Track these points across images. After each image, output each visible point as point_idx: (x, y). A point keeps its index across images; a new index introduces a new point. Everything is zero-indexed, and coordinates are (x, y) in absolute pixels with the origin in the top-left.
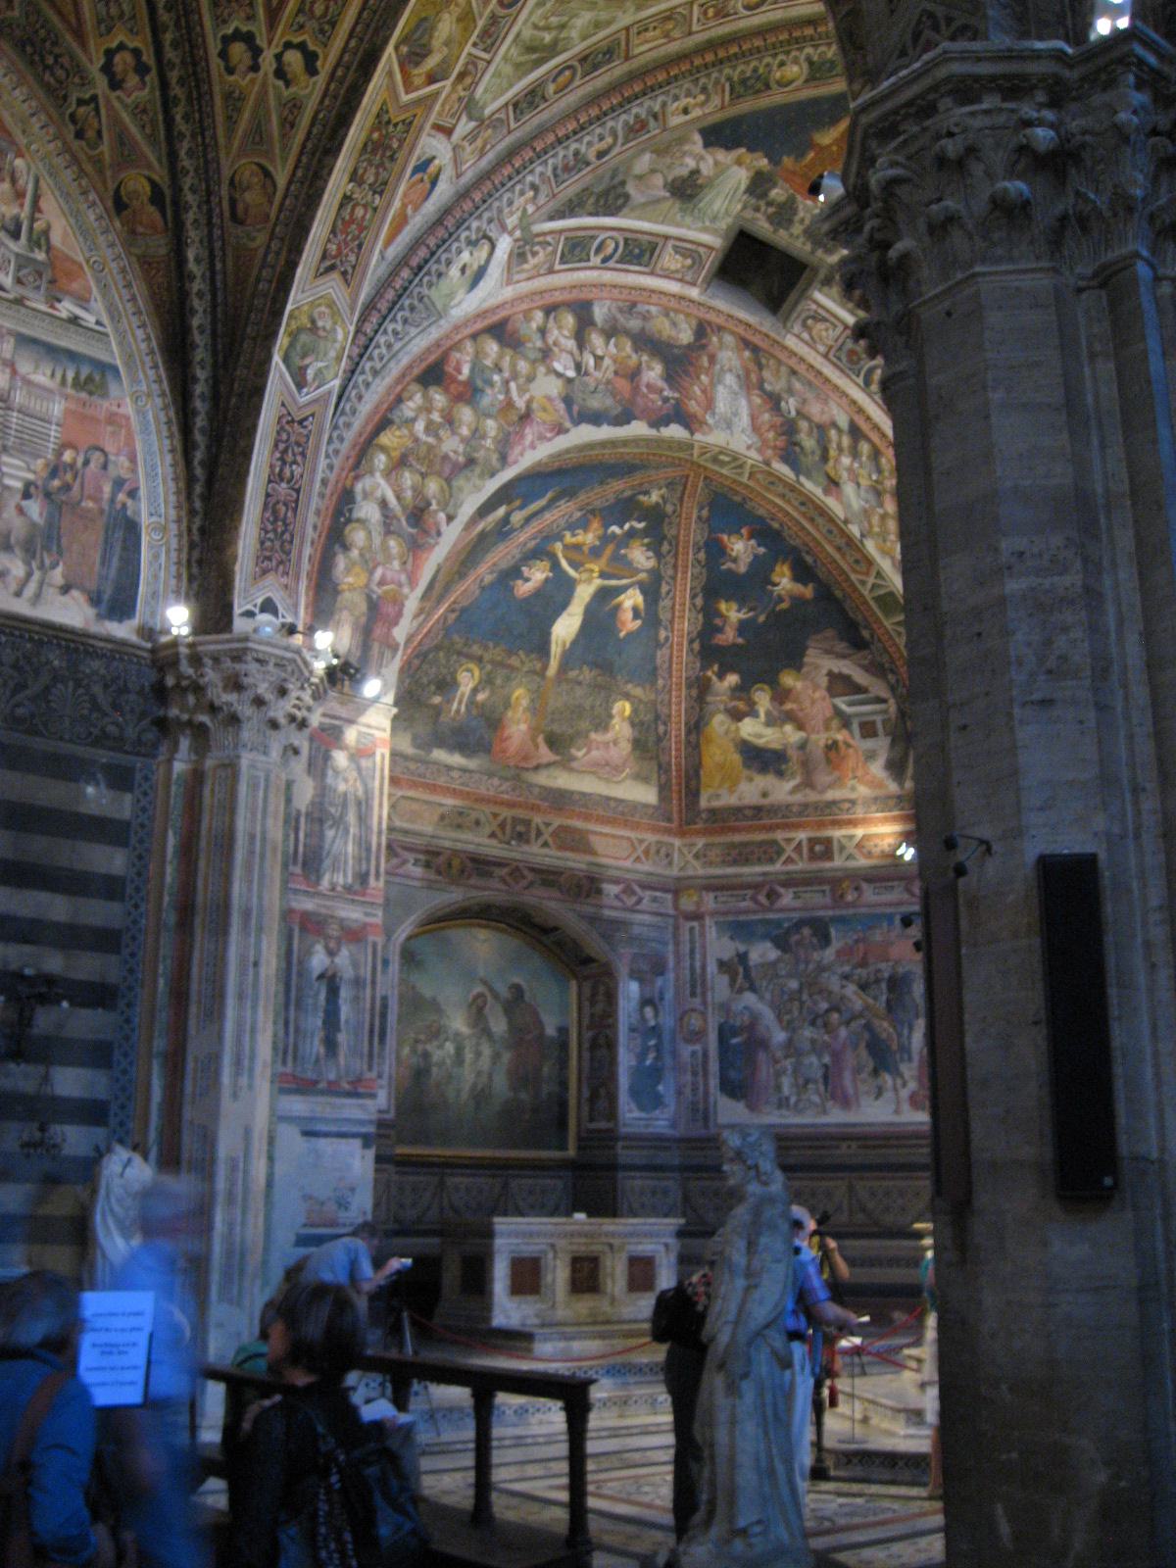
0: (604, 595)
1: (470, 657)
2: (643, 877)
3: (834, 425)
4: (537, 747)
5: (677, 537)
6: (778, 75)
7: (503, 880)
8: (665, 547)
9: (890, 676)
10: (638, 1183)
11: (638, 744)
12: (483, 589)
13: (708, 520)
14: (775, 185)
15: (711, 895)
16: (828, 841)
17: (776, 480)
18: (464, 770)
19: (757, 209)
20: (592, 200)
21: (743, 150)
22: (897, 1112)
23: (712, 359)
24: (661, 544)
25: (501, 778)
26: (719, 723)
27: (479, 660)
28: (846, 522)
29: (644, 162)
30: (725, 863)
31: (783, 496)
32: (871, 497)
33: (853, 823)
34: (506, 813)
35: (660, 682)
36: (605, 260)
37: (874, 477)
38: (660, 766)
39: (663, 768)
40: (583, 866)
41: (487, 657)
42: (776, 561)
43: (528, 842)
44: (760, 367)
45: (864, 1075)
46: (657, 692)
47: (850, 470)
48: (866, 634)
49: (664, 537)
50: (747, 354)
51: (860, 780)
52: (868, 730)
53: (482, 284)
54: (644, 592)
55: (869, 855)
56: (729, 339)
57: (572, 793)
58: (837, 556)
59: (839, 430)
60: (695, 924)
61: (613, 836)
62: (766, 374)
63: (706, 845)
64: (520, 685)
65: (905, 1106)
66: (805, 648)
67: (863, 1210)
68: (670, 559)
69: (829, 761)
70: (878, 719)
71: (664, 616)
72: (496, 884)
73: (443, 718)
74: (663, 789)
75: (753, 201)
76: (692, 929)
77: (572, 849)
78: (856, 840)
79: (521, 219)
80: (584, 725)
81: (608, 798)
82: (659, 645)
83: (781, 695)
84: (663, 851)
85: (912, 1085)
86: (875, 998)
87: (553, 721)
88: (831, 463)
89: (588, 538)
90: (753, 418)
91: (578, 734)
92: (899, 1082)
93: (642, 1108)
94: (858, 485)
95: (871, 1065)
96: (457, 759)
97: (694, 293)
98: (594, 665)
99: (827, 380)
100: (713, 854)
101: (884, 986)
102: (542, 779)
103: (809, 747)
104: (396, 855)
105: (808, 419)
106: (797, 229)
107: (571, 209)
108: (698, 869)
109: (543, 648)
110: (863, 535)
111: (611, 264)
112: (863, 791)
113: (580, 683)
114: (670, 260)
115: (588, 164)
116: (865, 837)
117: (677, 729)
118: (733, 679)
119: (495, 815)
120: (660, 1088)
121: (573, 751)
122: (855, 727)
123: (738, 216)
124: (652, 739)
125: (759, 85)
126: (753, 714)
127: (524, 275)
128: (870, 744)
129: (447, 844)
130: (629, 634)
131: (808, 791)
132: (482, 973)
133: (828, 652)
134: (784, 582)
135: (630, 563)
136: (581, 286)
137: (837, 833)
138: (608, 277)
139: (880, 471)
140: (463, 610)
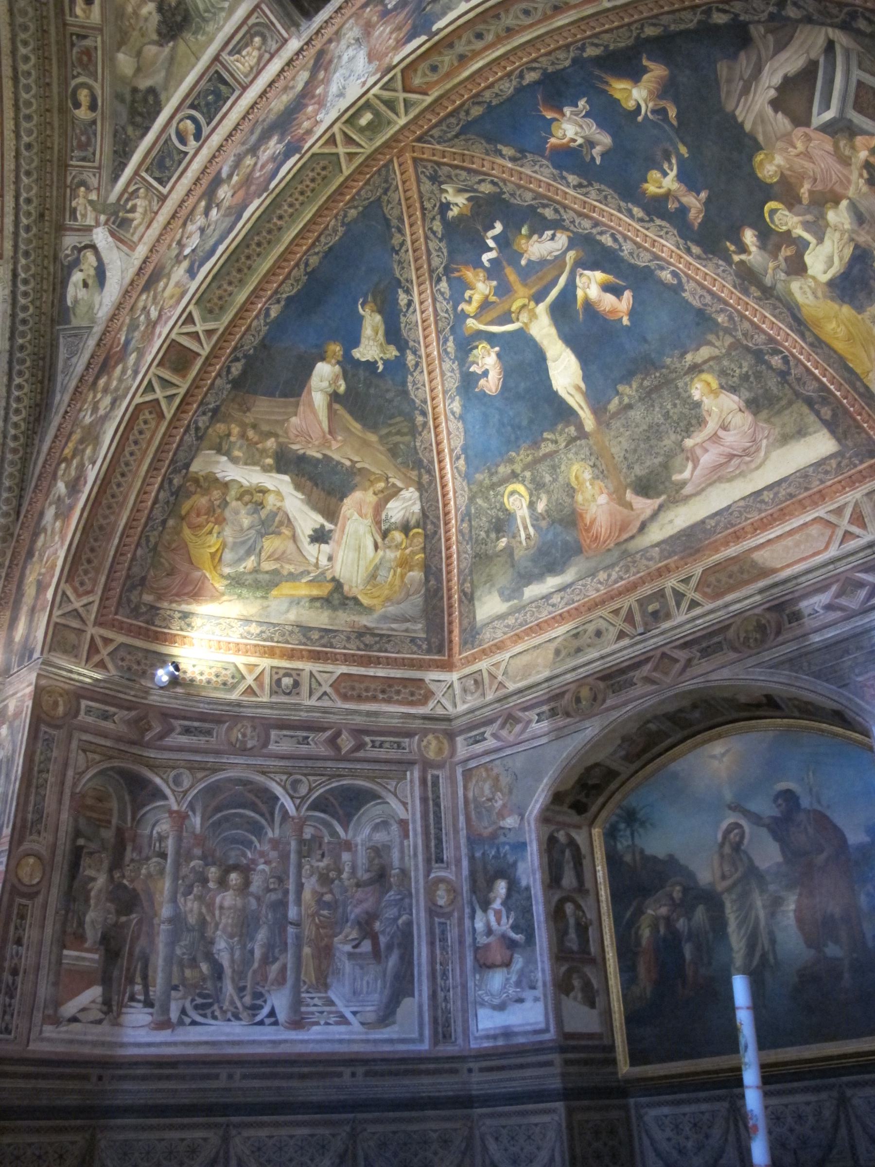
0: (563, 311)
1: (505, 481)
4: (629, 506)
5: (537, 196)
7: (648, 680)
8: (548, 213)
11: (754, 405)
12: (461, 418)
13: (522, 151)
18: (562, 589)
20: (130, 130)
24: (543, 217)
25: (606, 568)
27: (514, 476)
29: (125, 62)
31: (463, 59)
34: (629, 601)
36: (197, 136)
38: (810, 402)
40: (758, 598)
41: (518, 468)
42: (605, 92)
43: (668, 616)
46: (727, 331)
49: (532, 209)
53: (108, 274)
57: (703, 522)
61: (790, 533)
64: (569, 467)
66: (734, 117)
71: (642, 261)
72: (640, 689)
73: (519, 554)
77: (731, 589)
79: (95, 209)
80: (669, 441)
81: (759, 493)
82: (678, 288)
83: (786, 191)
87: (630, 467)
89: (481, 288)
91: (670, 456)
96: (552, 582)
97: (294, 44)
98: (627, 377)
102: (656, 534)
104: (517, 721)
107: (122, 154)
109: (563, 412)
111: (206, 131)
113: (630, 407)
114: (241, 64)
115: (94, 122)
117: (793, 343)
118: (749, 236)
119: (616, 612)
121: (676, 477)
124: (772, 382)
127: (142, 229)
129: (569, 677)
130: (632, 313)
132: (728, 796)
133: (746, 91)
135: (543, 263)
136: (203, 172)
138: (216, 139)
140: (465, 449)
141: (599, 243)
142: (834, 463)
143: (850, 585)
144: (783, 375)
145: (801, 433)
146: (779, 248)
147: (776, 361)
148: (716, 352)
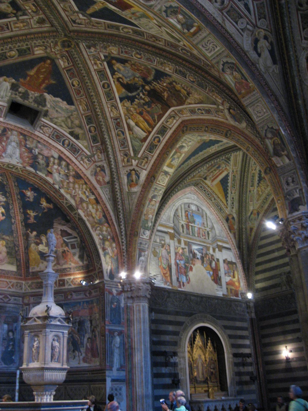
2: (11, 293)
3: (53, 157)
5: (10, 192)
6: (9, 54)
8: (8, 195)
9: (77, 231)
10: (3, 387)
11: (8, 253)
13: (18, 186)
14: (20, 87)
15: (33, 298)
16: (64, 280)
17: (30, 173)
19: (16, 94)
21: (5, 77)
22: (79, 363)
23: (8, 138)
24: (6, 194)
26: (33, 246)
28: (54, 184)
30: (37, 288)
31: (34, 177)
32: (64, 177)
33: (70, 275)
35: (15, 235)
37: (66, 171)
38: (17, 260)
39: (18, 260)
44: (26, 140)
45: (70, 352)
46: (14, 238)
47: (57, 170)
48: (68, 218)
49: (6, 192)
50: (21, 137)
51: (72, 262)
52: (73, 247)
54: (4, 208)
55: (75, 284)
56: (15, 133)
58: (54, 194)
59: (54, 158)
60: (27, 307)
62: (28, 142)
63: (32, 283)
65: (82, 362)
67: (69, 395)
68: (10, 198)
69: (63, 256)
70: (75, 243)
71: (12, 215)
74: (18, 267)
75: (14, 92)
76: (27, 308)
78: (71, 280)
82: (12, 224)
84: (19, 285)
85: (84, 355)
86: (75, 328)
88: (50, 167)
90: (21, 155)
92: (80, 354)
93: (5, 364)
94: (60, 174)
95: (73, 349)
99: (50, 144)
100: (33, 285)
101: (77, 324)
103: (58, 252)
105: (42, 155)
106: (31, 100)
108: (30, 290)
110: (60, 188)
112: (73, 265)
116: (74, 279)
117: (22, 248)
118: (35, 233)
120: (13, 357)
122: (70, 246)
123: (10, 97)
124: (14, 251)
125: (4, 58)
126: (42, 244)
128: (74, 251)
131: (58, 266)
133: (60, 224)
134: (44, 204)
137: (66, 278)
139: (69, 170)
141: (9, 206)
142: (14, 273)
143: (6, 297)
144: (16, 252)
145: (12, 264)
146: (38, 239)
147: (17, 249)
148: (9, 239)
